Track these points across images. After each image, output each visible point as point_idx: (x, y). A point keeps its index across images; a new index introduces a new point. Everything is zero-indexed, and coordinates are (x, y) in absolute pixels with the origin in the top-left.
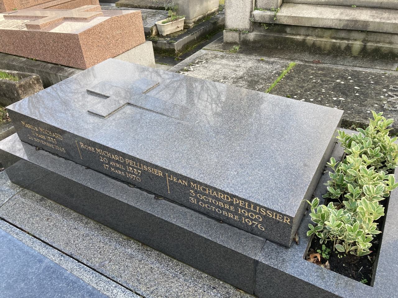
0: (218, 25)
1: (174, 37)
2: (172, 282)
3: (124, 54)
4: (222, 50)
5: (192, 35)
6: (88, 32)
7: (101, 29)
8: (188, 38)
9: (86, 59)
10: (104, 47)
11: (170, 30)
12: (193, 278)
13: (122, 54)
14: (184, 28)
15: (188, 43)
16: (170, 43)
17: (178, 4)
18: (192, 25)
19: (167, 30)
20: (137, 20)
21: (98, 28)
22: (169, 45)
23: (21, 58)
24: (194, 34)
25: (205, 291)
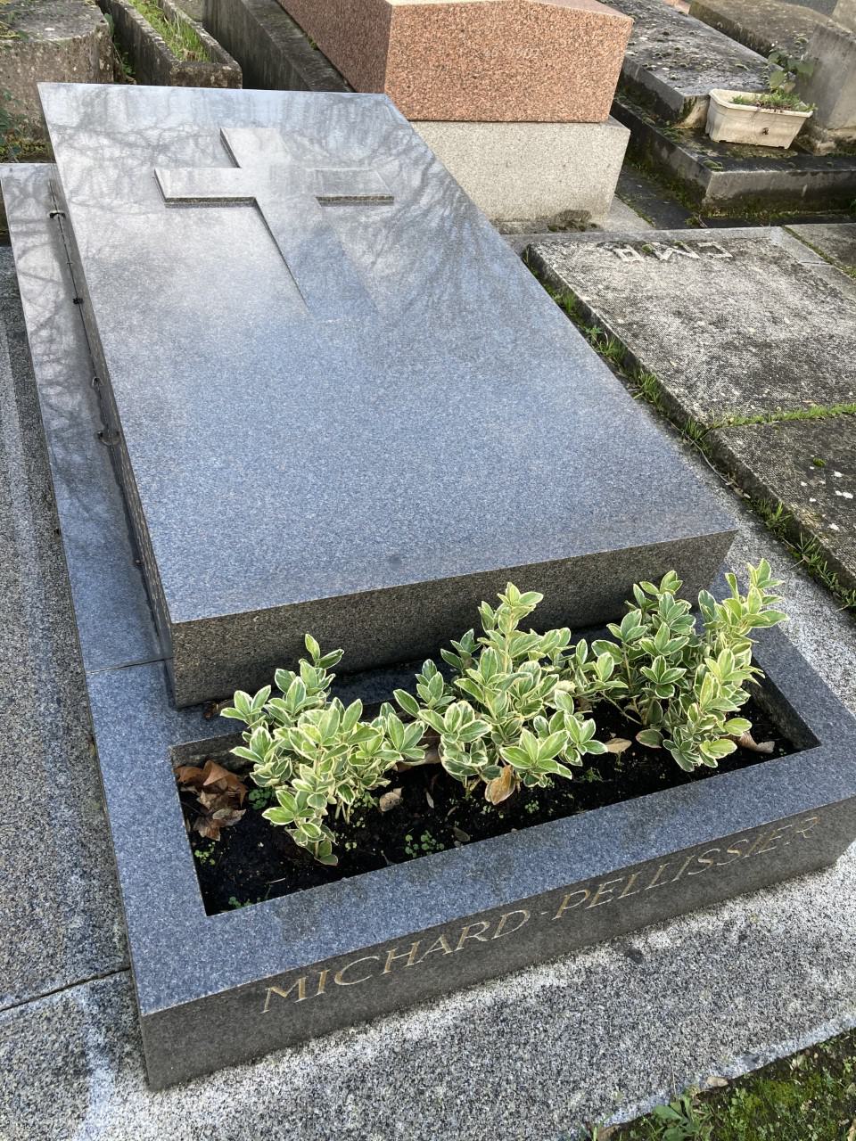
0: (816, 154)
1: (732, 154)
2: (12, 633)
3: (516, 126)
4: (834, 256)
5: (794, 174)
6: (427, 14)
7: (470, 22)
8: (774, 176)
9: (389, 89)
10: (460, 77)
11: (739, 132)
12: (50, 655)
13: (512, 126)
14: (793, 146)
15: (764, 193)
16: (703, 168)
17: (821, 63)
18: (825, 145)
19: (728, 126)
20: (606, 44)
21: (464, 15)
22: (698, 169)
23: (296, 31)
24: (803, 174)
25: (36, 692)
